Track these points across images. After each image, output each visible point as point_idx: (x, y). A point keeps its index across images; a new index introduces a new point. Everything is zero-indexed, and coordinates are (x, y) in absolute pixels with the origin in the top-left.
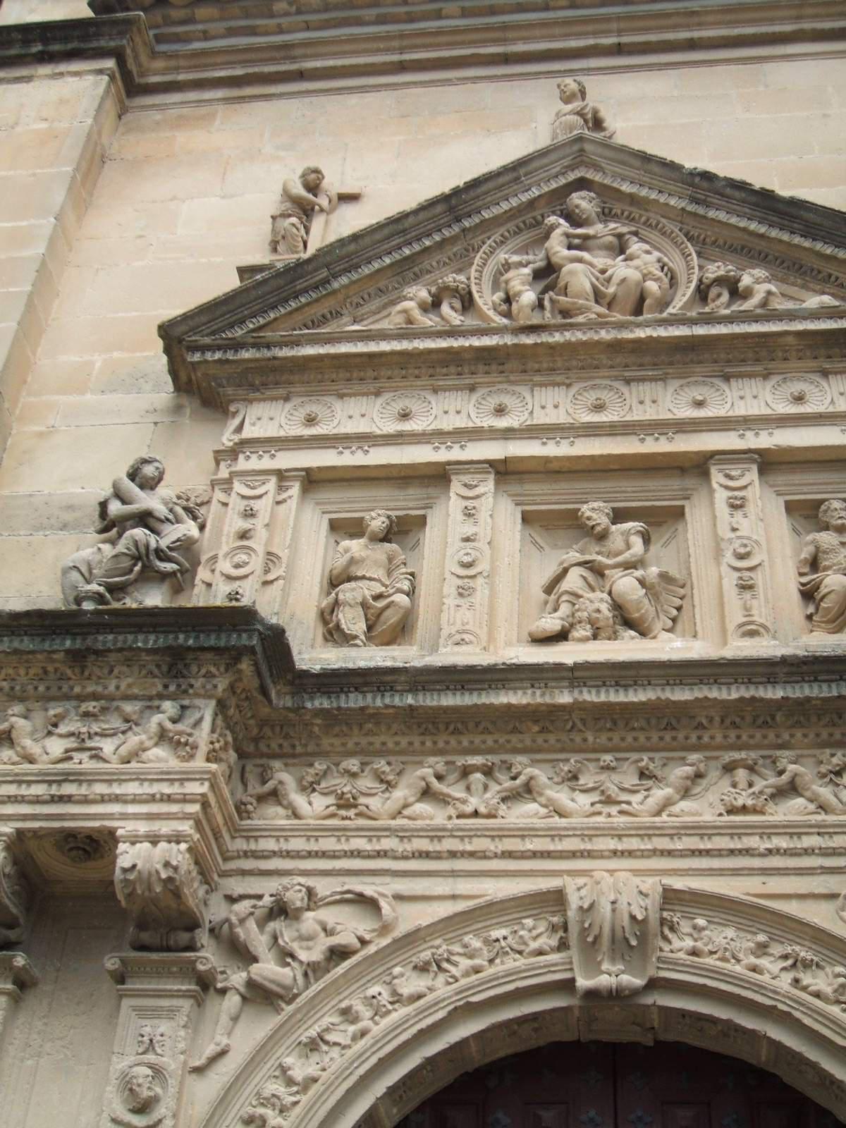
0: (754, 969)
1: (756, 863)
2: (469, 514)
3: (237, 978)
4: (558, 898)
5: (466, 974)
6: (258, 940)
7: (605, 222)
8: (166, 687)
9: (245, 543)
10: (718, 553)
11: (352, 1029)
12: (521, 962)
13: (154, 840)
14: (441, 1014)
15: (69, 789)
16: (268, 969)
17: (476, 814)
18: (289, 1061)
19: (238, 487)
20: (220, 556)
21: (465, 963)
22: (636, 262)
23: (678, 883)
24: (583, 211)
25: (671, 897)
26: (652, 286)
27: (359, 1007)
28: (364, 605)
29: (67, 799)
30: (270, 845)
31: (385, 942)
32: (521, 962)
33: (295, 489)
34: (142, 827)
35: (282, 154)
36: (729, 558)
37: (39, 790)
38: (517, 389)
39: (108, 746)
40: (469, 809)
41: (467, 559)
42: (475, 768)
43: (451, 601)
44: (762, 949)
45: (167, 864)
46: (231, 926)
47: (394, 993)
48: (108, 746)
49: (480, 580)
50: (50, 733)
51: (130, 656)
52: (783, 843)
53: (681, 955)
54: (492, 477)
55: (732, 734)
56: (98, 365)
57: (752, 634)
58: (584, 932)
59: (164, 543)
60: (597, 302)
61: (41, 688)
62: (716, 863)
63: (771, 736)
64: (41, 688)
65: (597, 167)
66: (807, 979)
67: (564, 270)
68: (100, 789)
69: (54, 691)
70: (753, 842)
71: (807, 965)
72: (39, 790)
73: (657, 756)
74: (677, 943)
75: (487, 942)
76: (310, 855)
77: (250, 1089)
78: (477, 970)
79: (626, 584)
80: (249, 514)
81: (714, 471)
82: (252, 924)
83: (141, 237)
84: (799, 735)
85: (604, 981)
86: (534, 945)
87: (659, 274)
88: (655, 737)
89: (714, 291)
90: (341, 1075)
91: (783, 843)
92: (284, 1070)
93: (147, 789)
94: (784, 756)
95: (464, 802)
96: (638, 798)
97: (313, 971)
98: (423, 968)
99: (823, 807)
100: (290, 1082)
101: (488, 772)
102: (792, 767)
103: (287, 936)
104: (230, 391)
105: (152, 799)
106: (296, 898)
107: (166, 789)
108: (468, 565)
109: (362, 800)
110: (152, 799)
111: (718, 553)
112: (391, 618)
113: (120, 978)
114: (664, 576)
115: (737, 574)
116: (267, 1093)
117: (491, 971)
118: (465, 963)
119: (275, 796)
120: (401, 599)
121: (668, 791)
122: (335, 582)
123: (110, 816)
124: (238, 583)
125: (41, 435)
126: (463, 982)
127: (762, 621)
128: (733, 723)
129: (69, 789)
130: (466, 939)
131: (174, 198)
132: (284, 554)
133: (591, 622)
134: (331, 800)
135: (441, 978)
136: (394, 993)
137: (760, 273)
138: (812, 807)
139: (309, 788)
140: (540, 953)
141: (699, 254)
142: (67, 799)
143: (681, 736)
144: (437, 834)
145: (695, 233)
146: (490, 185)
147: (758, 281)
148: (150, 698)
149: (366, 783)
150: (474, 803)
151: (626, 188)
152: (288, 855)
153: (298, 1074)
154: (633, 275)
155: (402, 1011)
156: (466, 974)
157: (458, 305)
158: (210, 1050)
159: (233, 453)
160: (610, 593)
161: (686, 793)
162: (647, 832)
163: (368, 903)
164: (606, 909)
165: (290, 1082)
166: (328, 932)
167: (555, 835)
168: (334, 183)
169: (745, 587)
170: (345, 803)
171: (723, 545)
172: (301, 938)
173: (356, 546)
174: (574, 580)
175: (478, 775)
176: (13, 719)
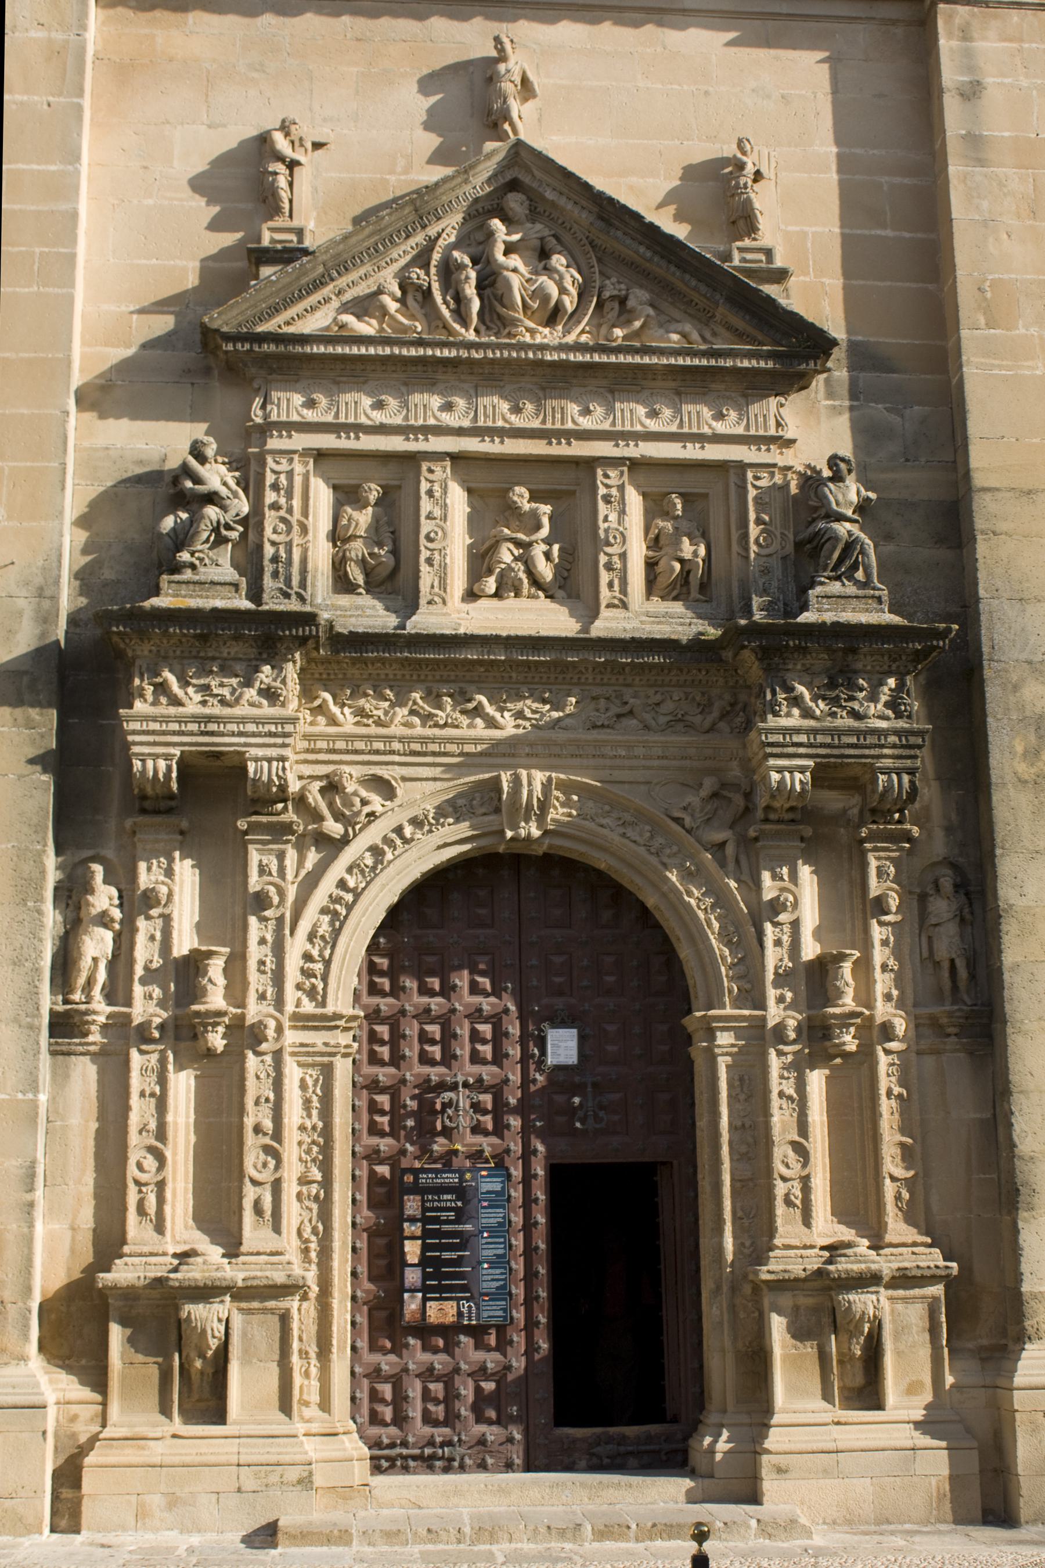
1: (608, 762)
8: (260, 654)
15: (213, 727)
29: (212, 734)
35: (255, 75)
37: (193, 727)
38: (466, 386)
51: (237, 638)
55: (599, 677)
57: (615, 606)
59: (229, 517)
61: (178, 653)
63: (621, 678)
64: (178, 653)
65: (529, 171)
66: (630, 833)
68: (233, 727)
69: (186, 654)
72: (193, 727)
73: (554, 687)
84: (637, 679)
86: (483, 810)
88: (553, 676)
89: (608, 306)
94: (628, 693)
99: (647, 727)
102: (632, 701)
104: (253, 370)
112: (384, 572)
128: (601, 673)
129: (213, 727)
141: (600, 260)
142: (212, 734)
143: (568, 676)
144: (424, 740)
145: (599, 242)
146: (447, 186)
148: (250, 660)
151: (549, 195)
157: (420, 297)
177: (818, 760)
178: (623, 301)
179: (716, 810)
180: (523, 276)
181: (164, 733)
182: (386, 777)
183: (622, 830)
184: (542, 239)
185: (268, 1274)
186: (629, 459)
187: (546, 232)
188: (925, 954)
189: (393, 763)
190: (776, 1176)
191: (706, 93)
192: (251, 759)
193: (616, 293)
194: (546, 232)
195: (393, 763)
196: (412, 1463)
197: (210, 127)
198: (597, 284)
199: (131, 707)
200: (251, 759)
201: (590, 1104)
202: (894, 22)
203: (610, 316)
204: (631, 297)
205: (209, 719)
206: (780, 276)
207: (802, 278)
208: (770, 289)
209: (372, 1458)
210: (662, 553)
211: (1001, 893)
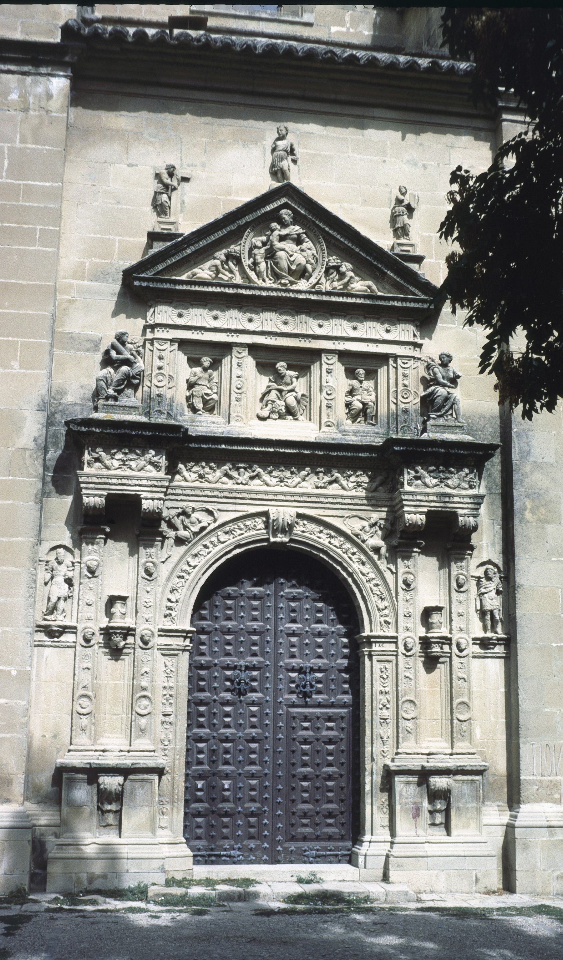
0: (319, 537)
2: (239, 365)
3: (172, 534)
4: (266, 514)
5: (239, 535)
6: (177, 522)
7: (294, 225)
9: (161, 371)
10: (321, 390)
11: (207, 550)
12: (255, 532)
13: (153, 499)
14: (232, 547)
16: (182, 533)
17: (242, 483)
18: (189, 559)
19: (156, 344)
20: (153, 375)
21: (239, 532)
22: (304, 253)
23: (301, 511)
24: (286, 221)
25: (299, 516)
26: (309, 267)
27: (209, 544)
28: (202, 397)
30: (179, 491)
31: (217, 524)
32: (255, 532)
33: (176, 346)
34: (149, 495)
35: (153, 140)
36: (324, 394)
39: (133, 464)
40: (239, 482)
41: (239, 386)
42: (241, 468)
43: (233, 402)
44: (321, 532)
45: (158, 508)
46: (170, 519)
47: (218, 540)
48: (133, 464)
49: (243, 395)
50: (112, 458)
52: (331, 500)
53: (299, 532)
54: (247, 349)
56: (87, 264)
57: (329, 426)
58: (273, 526)
60: (289, 274)
62: (311, 505)
66: (332, 541)
67: (277, 254)
70: (322, 499)
71: (333, 537)
74: (298, 528)
75: (244, 525)
76: (192, 495)
77: (179, 567)
78: (242, 534)
79: (291, 399)
80: (161, 358)
81: (323, 355)
82: (176, 518)
83: (94, 185)
85: (278, 539)
86: (259, 527)
87: (313, 261)
89: (332, 271)
90: (204, 565)
91: (331, 500)
92: (188, 563)
93: (150, 483)
95: (238, 479)
96: (290, 481)
97: (196, 534)
98: (226, 533)
100: (190, 566)
101: (245, 469)
103: (187, 522)
105: (151, 486)
106: (189, 510)
107: (156, 484)
108: (239, 389)
109: (206, 476)
110: (151, 486)
111: (321, 390)
113: (138, 536)
114: (303, 395)
115: (326, 402)
116: (184, 569)
117: (246, 535)
118: (239, 532)
119: (179, 473)
120: (215, 397)
121: (299, 479)
122: (191, 385)
123: (138, 491)
124: (160, 389)
125: (70, 301)
126: (238, 538)
127: (332, 421)
129: (124, 481)
130: (239, 524)
131: (105, 162)
132: (174, 376)
133: (279, 413)
134: (196, 475)
135: (232, 536)
136: (218, 540)
137: (350, 266)
138: (340, 487)
139: (189, 470)
140: (260, 529)
144: (231, 491)
147: (348, 270)
149: (207, 469)
150: (241, 479)
152: (185, 495)
153: (192, 564)
154: (303, 261)
155: (222, 546)
156: (239, 535)
158: (166, 556)
159: (153, 327)
160: (285, 401)
161: (304, 480)
162: (293, 494)
163: (210, 513)
164: (281, 521)
165: (190, 566)
166: (200, 522)
167: (266, 493)
168: (180, 173)
169: (329, 407)
170: (201, 477)
171: (323, 388)
172: (191, 523)
173: (198, 370)
174: (273, 395)
175: (242, 470)
176: (100, 453)
177: (429, 509)
178: (337, 268)
179: (376, 531)
180: (287, 252)
181: (100, 483)
182: (211, 509)
183: (329, 539)
184: (299, 235)
185: (145, 762)
186: (339, 351)
187: (301, 231)
188: (479, 608)
189: (215, 502)
190: (400, 717)
191: (384, 161)
192: (144, 498)
193: (335, 264)
194: (301, 231)
195: (215, 502)
196: (213, 858)
197: (128, 166)
198: (326, 260)
199: (82, 469)
200: (144, 498)
201: (308, 678)
202: (480, 129)
203: (331, 276)
204: (343, 266)
205: (123, 477)
206: (419, 260)
207: (429, 260)
208: (414, 267)
209: (194, 856)
210: (354, 398)
211: (517, 579)
